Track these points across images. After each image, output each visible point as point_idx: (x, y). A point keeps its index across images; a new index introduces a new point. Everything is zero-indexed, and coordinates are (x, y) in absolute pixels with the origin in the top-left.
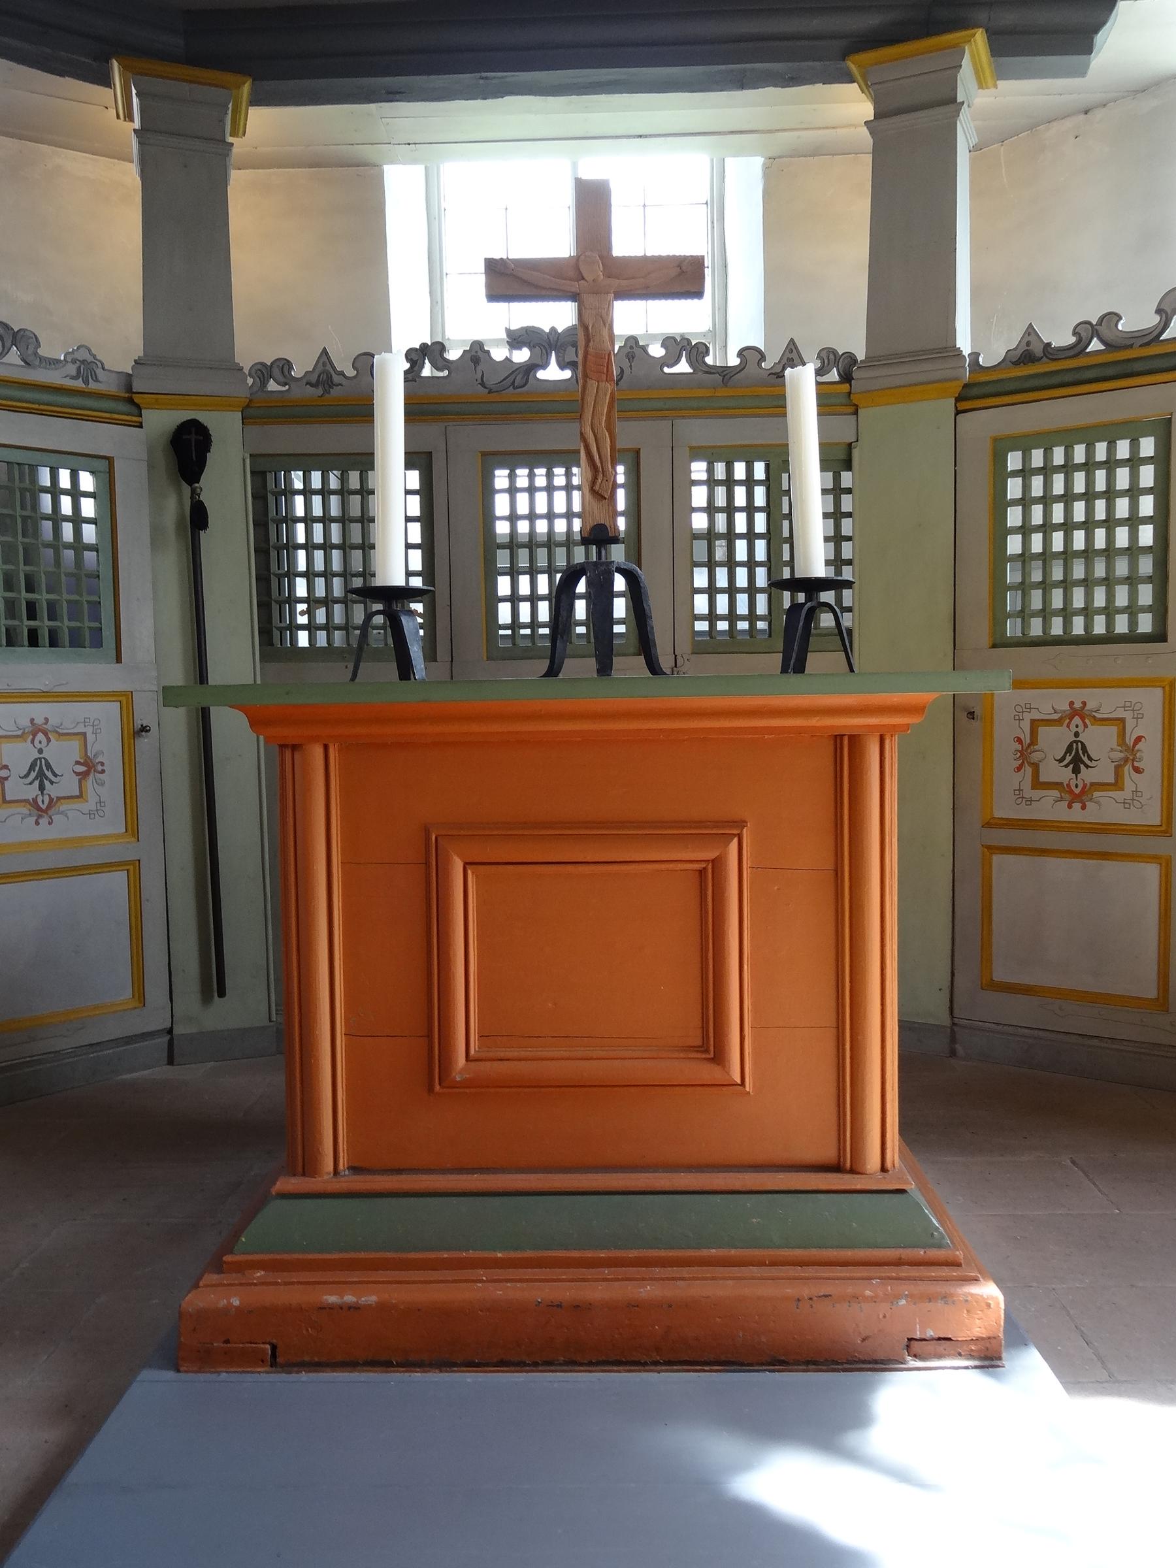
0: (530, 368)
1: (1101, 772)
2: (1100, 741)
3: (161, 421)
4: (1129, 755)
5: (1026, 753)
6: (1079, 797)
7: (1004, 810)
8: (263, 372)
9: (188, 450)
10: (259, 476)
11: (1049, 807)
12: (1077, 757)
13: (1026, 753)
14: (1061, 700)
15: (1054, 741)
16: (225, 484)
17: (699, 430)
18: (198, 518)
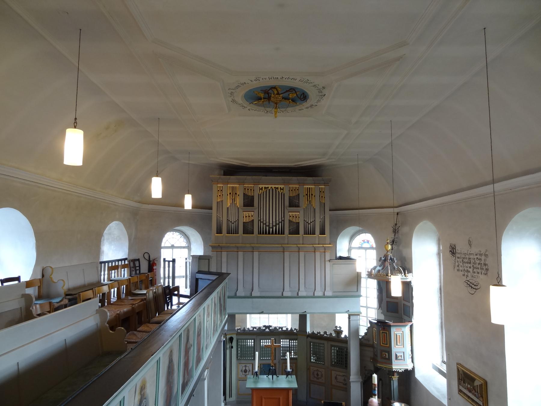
0: (265, 330)
1: (320, 376)
2: (319, 373)
3: (228, 337)
4: (322, 376)
5: (313, 373)
6: (318, 379)
7: (312, 379)
8: (238, 329)
9: (231, 339)
10: (237, 341)
11: (315, 379)
12: (318, 375)
13: (313, 373)
14: (316, 369)
15: (316, 373)
16: (234, 344)
17: (282, 337)
18: (232, 347)
